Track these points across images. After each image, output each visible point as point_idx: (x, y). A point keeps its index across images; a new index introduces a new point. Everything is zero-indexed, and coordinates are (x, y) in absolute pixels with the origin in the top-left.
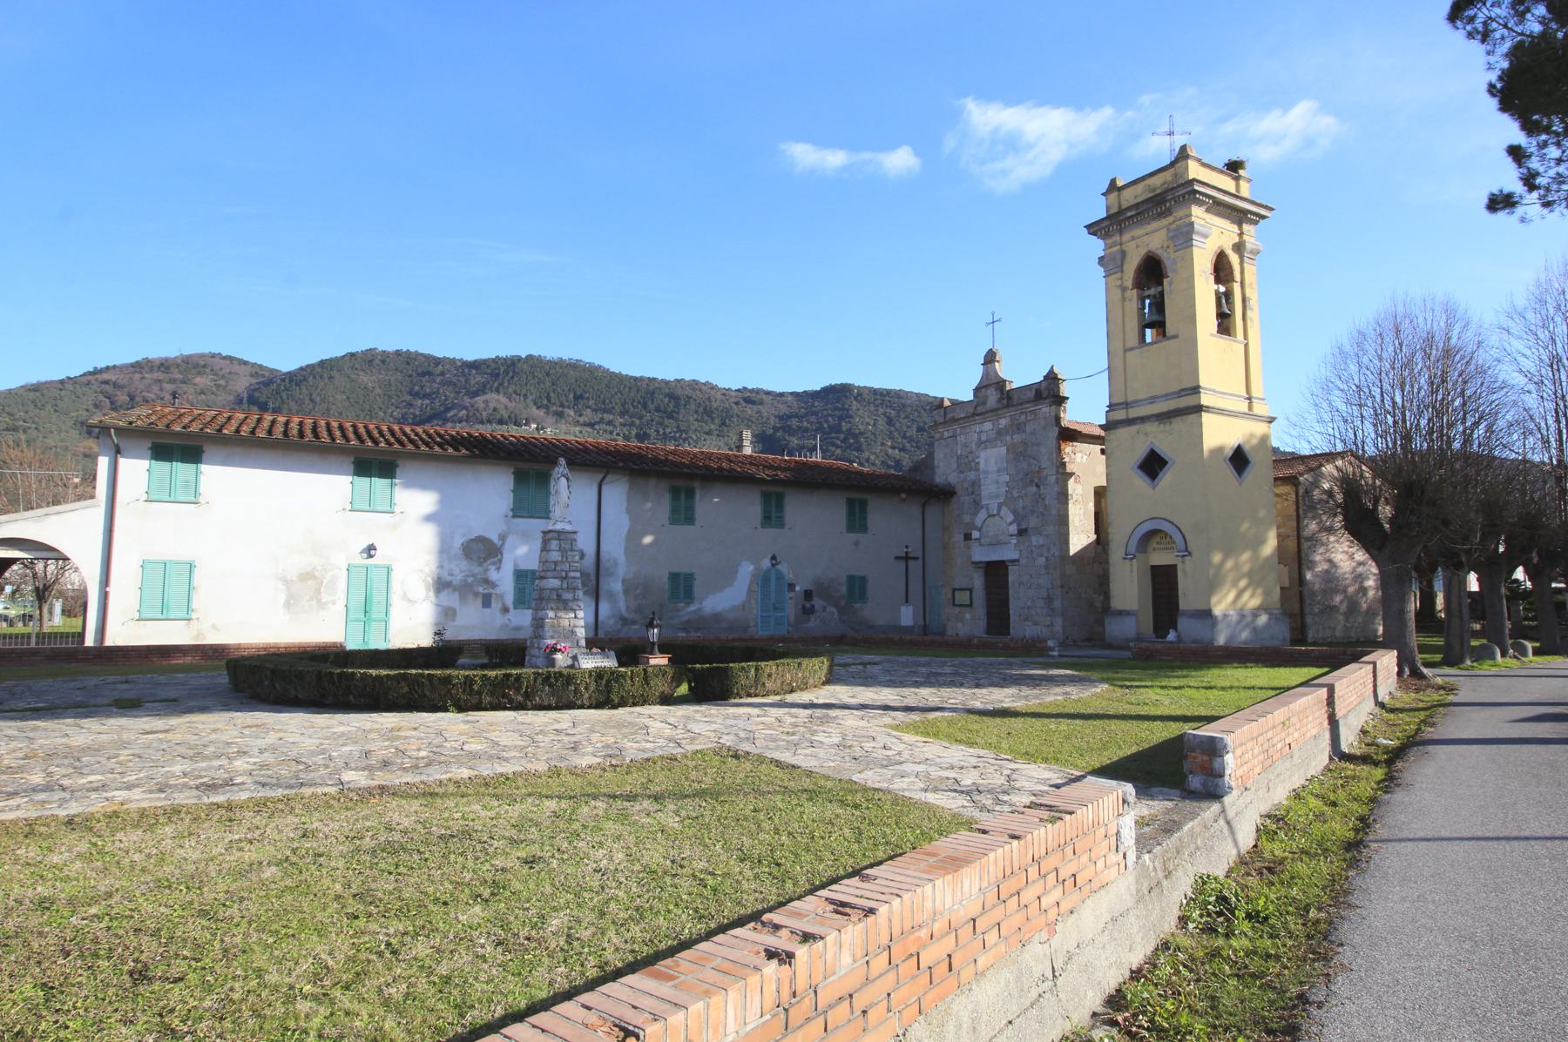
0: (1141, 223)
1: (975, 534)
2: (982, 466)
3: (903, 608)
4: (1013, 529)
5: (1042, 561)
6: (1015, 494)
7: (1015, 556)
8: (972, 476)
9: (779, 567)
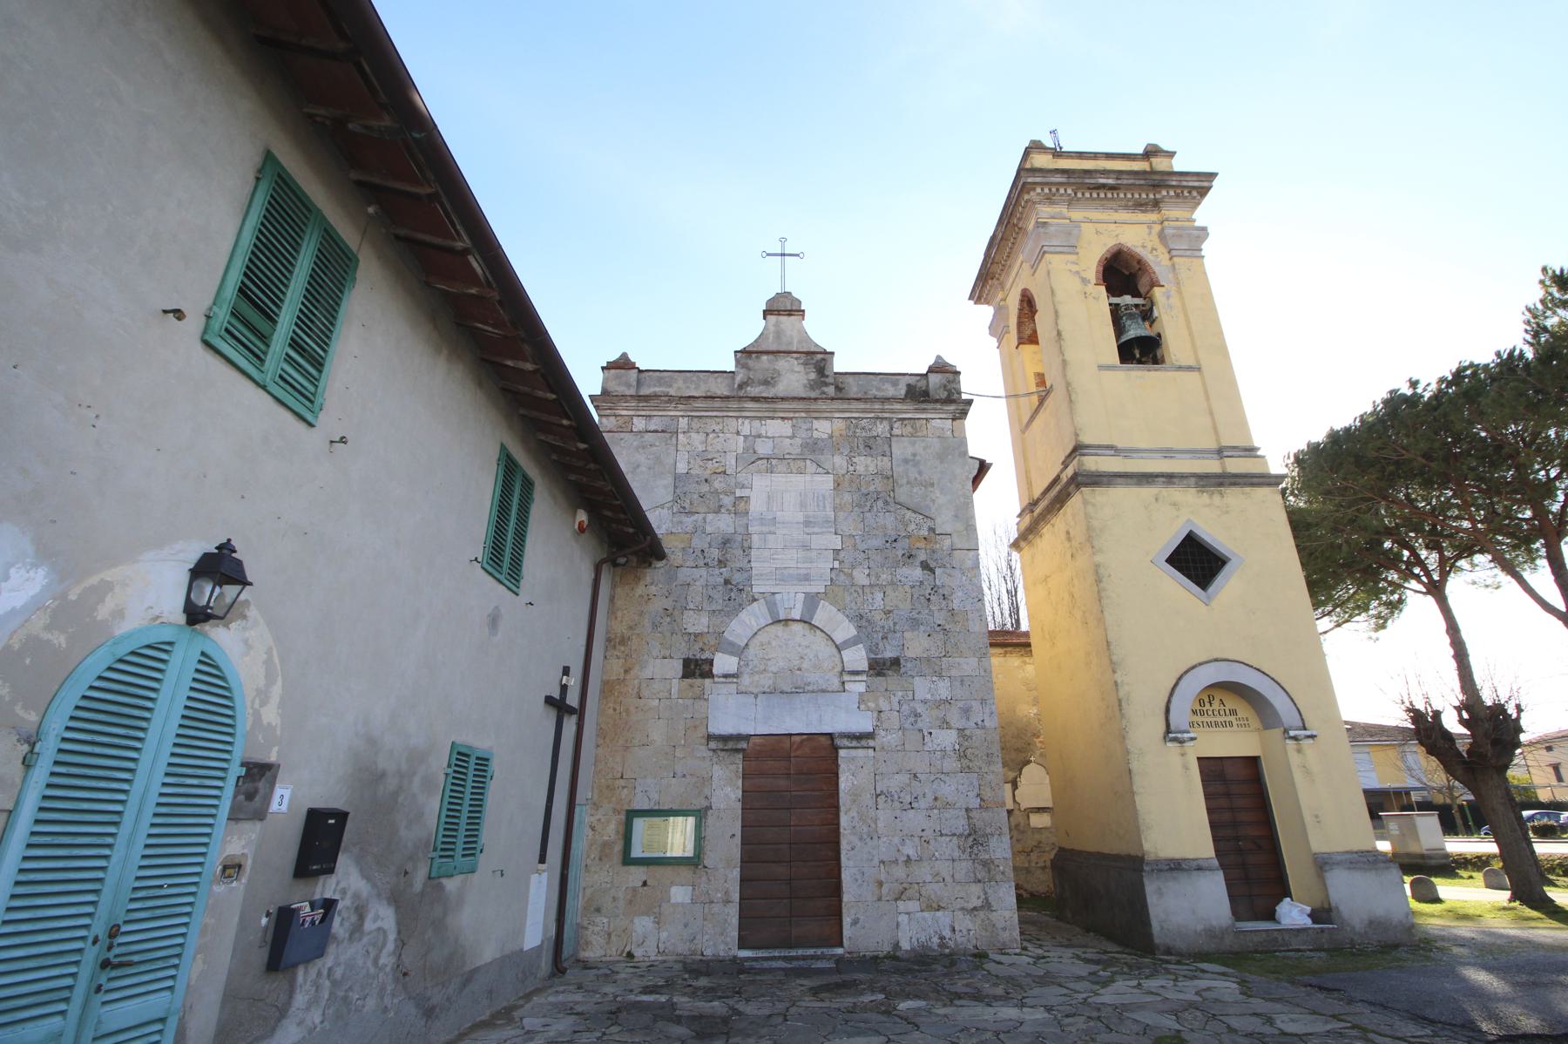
0: (1103, 204)
1: (724, 663)
2: (756, 506)
3: (534, 877)
4: (857, 657)
5: (947, 738)
6: (861, 577)
7: (864, 724)
8: (723, 524)
9: (224, 639)
